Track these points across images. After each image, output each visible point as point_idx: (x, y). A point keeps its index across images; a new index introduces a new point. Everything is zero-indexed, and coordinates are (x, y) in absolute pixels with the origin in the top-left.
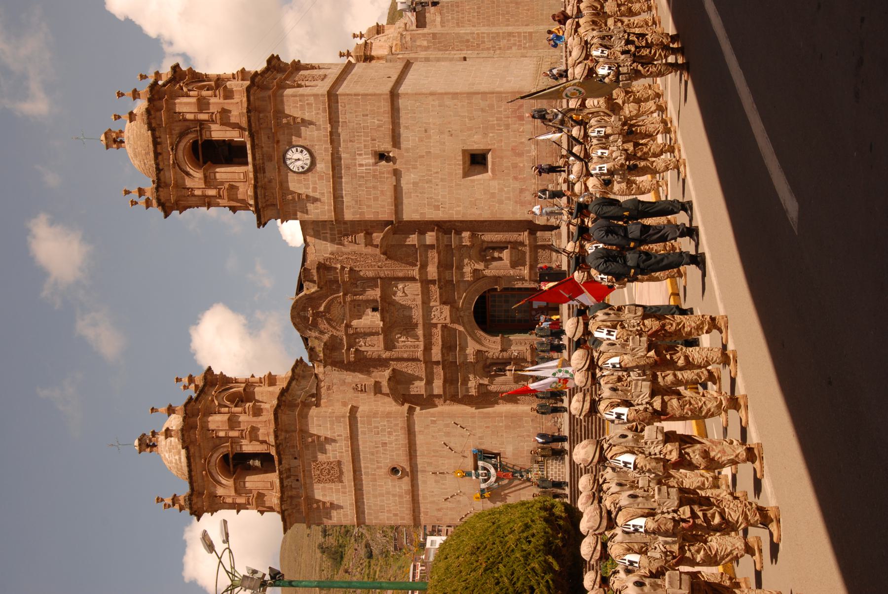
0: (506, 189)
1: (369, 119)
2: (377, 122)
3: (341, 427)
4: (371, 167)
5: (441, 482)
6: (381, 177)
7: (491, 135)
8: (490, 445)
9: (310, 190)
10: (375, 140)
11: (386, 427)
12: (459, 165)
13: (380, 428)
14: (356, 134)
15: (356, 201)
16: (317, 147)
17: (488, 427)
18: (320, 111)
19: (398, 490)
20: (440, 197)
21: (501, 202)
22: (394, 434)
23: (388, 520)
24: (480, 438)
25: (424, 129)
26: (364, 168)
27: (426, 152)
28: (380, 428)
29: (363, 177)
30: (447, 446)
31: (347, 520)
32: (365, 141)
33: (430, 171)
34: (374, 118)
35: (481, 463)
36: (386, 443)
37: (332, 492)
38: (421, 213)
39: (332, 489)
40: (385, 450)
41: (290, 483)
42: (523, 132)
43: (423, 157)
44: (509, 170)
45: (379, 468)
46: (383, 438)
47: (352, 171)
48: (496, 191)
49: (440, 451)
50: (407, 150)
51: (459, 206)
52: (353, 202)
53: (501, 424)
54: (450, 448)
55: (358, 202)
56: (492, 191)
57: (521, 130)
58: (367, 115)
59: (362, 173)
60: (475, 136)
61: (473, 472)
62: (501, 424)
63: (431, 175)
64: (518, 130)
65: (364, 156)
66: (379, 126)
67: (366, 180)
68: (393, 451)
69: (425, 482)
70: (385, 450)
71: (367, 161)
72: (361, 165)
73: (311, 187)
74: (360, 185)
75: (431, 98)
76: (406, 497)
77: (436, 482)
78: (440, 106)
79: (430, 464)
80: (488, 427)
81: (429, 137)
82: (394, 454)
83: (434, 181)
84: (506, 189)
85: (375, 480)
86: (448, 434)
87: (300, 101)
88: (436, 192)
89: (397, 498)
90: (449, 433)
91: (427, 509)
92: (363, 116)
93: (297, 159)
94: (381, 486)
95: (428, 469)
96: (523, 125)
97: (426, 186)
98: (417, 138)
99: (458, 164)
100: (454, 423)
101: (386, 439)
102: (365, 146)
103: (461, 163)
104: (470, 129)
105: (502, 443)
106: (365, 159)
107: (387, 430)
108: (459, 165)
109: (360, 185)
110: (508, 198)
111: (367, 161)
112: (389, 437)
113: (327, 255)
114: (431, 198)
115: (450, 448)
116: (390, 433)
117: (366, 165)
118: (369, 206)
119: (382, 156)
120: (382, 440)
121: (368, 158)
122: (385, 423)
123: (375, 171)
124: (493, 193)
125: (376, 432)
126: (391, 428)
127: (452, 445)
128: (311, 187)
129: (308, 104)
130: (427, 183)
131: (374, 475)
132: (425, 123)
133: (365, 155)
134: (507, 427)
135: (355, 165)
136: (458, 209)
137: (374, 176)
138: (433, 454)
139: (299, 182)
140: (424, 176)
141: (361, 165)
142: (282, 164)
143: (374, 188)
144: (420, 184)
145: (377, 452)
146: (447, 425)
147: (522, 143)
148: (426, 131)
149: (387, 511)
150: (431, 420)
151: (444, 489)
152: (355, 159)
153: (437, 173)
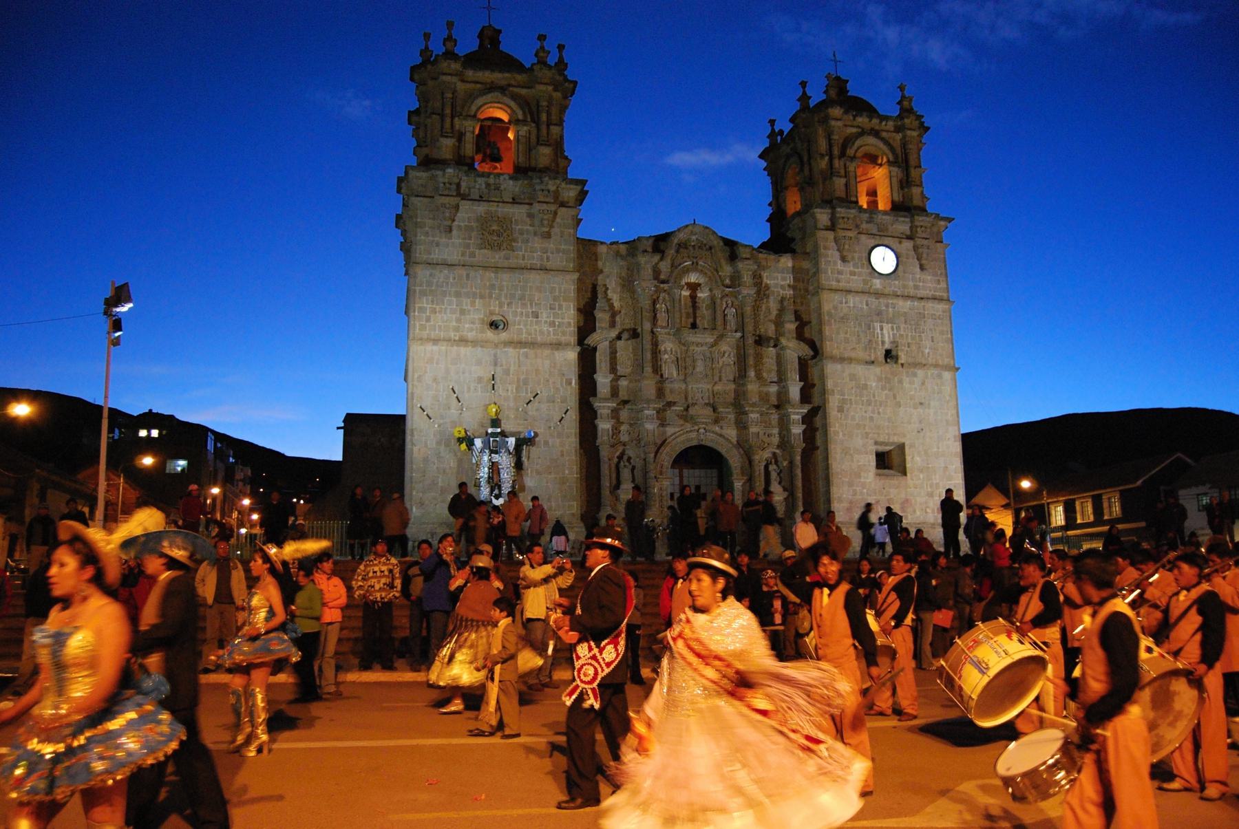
0: (865, 491)
1: (928, 343)
2: (927, 351)
3: (561, 262)
4: (880, 339)
5: (479, 386)
6: (870, 348)
7: (921, 476)
8: (532, 456)
9: (852, 269)
10: (909, 347)
11: (560, 320)
12: (889, 439)
13: (559, 312)
14: (914, 327)
15: (842, 318)
16: (897, 282)
17: (562, 455)
18: (932, 292)
19: (467, 326)
20: (852, 413)
21: (850, 484)
22: (551, 329)
23: (420, 308)
24: (546, 443)
25: (923, 401)
26: (879, 331)
27: (900, 402)
28: (559, 312)
29: (870, 329)
30: (534, 397)
31: (420, 254)
32: (907, 335)
33: (881, 405)
34: (930, 348)
35: (512, 441)
36: (537, 318)
37: (464, 239)
38: (833, 391)
39: (470, 239)
40: (527, 316)
41: (477, 187)
42: (926, 512)
43: (895, 397)
44: (885, 496)
45: (501, 306)
46: (545, 315)
47: (875, 318)
48: (862, 480)
49: (527, 389)
50: (900, 382)
51: (844, 435)
52: (842, 315)
53: (567, 472)
54: (531, 401)
55: (844, 319)
56: (862, 474)
57: (928, 510)
58: (933, 341)
59: (874, 328)
60: (918, 459)
61: (499, 430)
62: (567, 472)
63: (875, 406)
64: (928, 507)
65: (891, 333)
66: (923, 352)
67: (866, 332)
68: (525, 325)
69: (479, 363)
70: (527, 316)
71: (887, 335)
72: (882, 329)
73: (856, 270)
74: (860, 325)
75: (954, 412)
76: (455, 336)
77: (480, 380)
78: (947, 421)
79: (507, 372)
80: (562, 455)
81: (915, 408)
82: (522, 327)
83: (870, 408)
84: (865, 491)
85: (482, 297)
86: (551, 400)
87: (941, 274)
88: (858, 410)
89: (454, 324)
90: (553, 402)
91: (437, 363)
92: (932, 337)
93: (883, 260)
94: (473, 304)
95: (499, 369)
96: (933, 512)
97: (865, 399)
98: (912, 393)
99: (890, 438)
100: (567, 410)
101: (544, 316)
102: (902, 336)
103: (891, 441)
104: (926, 452)
105: (538, 473)
106: (889, 333)
107: (556, 320)
108: (889, 439)
109: (860, 325)
110: (855, 494)
111: (887, 335)
112: (546, 322)
113: (765, 280)
114: (851, 404)
115: (531, 401)
116: (552, 324)
117: (882, 334)
118: (838, 333)
119: (889, 355)
120: (541, 313)
121: (889, 337)
122: (566, 320)
123: (877, 342)
124: (860, 477)
125: (552, 306)
126: (559, 326)
127: (535, 404)
128: (856, 270)
129: (939, 280)
130: (867, 401)
131: (490, 297)
132: (929, 404)
133: (893, 334)
134: (563, 481)
135: (881, 322)
136: (841, 434)
137: (870, 341)
138: (522, 377)
139: (860, 258)
140: (874, 397)
141: (882, 329)
142: (877, 243)
143: (859, 341)
144: (865, 392)
145: (524, 305)
146: (564, 401)
147: (914, 511)
148: (921, 404)
149: (435, 309)
150: (571, 379)
151: (469, 388)
152: (887, 323)
153: (879, 413)
